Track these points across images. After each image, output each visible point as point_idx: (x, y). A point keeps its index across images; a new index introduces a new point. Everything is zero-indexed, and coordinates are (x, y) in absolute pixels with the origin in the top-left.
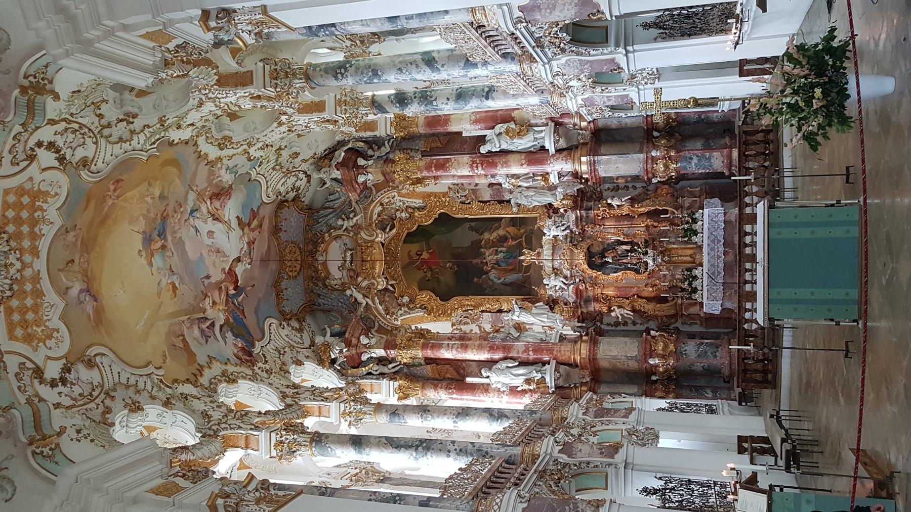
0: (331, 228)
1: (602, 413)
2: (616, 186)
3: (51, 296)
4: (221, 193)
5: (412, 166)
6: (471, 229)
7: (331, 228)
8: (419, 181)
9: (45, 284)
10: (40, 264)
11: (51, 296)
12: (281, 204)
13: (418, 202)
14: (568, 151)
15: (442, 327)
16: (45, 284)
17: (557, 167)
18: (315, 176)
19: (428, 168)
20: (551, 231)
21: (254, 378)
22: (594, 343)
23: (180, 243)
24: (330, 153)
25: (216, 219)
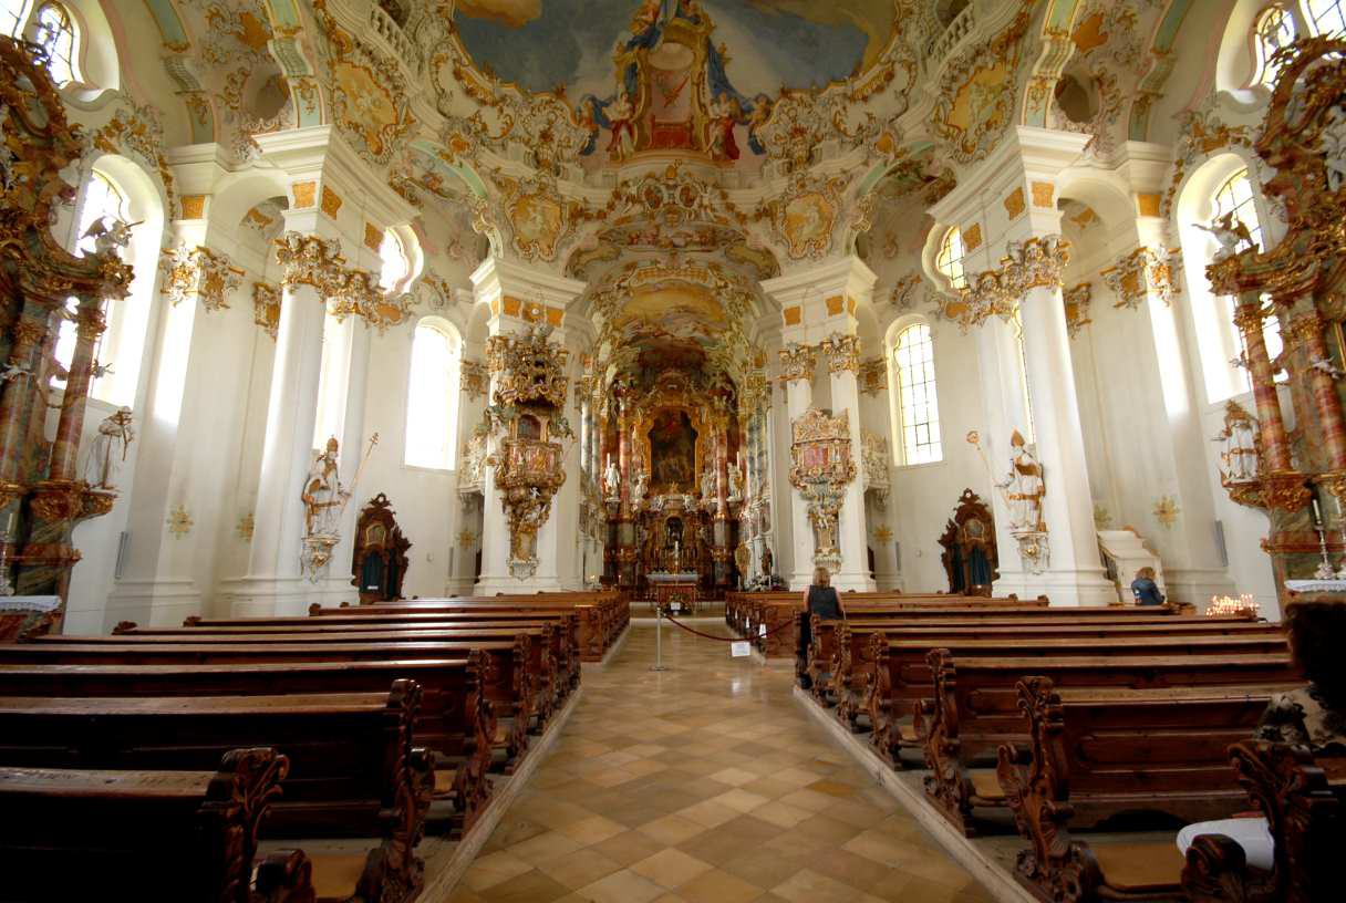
0: (689, 376)
1: (601, 526)
2: (711, 533)
3: (657, 280)
4: (707, 332)
5: (722, 425)
6: (689, 451)
7: (689, 376)
8: (714, 428)
9: (663, 278)
10: (673, 277)
11: (657, 280)
12: (703, 354)
13: (704, 420)
14: (728, 508)
15: (634, 435)
16: (663, 278)
17: (719, 501)
18: (718, 373)
19: (721, 435)
20: (687, 499)
21: (613, 350)
22: (631, 521)
23: (682, 317)
24: (729, 381)
25: (694, 330)
